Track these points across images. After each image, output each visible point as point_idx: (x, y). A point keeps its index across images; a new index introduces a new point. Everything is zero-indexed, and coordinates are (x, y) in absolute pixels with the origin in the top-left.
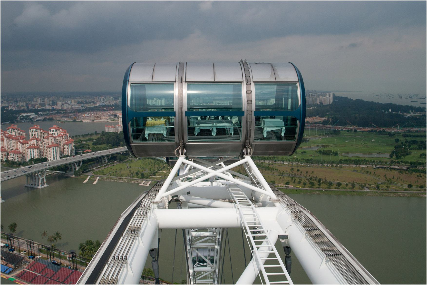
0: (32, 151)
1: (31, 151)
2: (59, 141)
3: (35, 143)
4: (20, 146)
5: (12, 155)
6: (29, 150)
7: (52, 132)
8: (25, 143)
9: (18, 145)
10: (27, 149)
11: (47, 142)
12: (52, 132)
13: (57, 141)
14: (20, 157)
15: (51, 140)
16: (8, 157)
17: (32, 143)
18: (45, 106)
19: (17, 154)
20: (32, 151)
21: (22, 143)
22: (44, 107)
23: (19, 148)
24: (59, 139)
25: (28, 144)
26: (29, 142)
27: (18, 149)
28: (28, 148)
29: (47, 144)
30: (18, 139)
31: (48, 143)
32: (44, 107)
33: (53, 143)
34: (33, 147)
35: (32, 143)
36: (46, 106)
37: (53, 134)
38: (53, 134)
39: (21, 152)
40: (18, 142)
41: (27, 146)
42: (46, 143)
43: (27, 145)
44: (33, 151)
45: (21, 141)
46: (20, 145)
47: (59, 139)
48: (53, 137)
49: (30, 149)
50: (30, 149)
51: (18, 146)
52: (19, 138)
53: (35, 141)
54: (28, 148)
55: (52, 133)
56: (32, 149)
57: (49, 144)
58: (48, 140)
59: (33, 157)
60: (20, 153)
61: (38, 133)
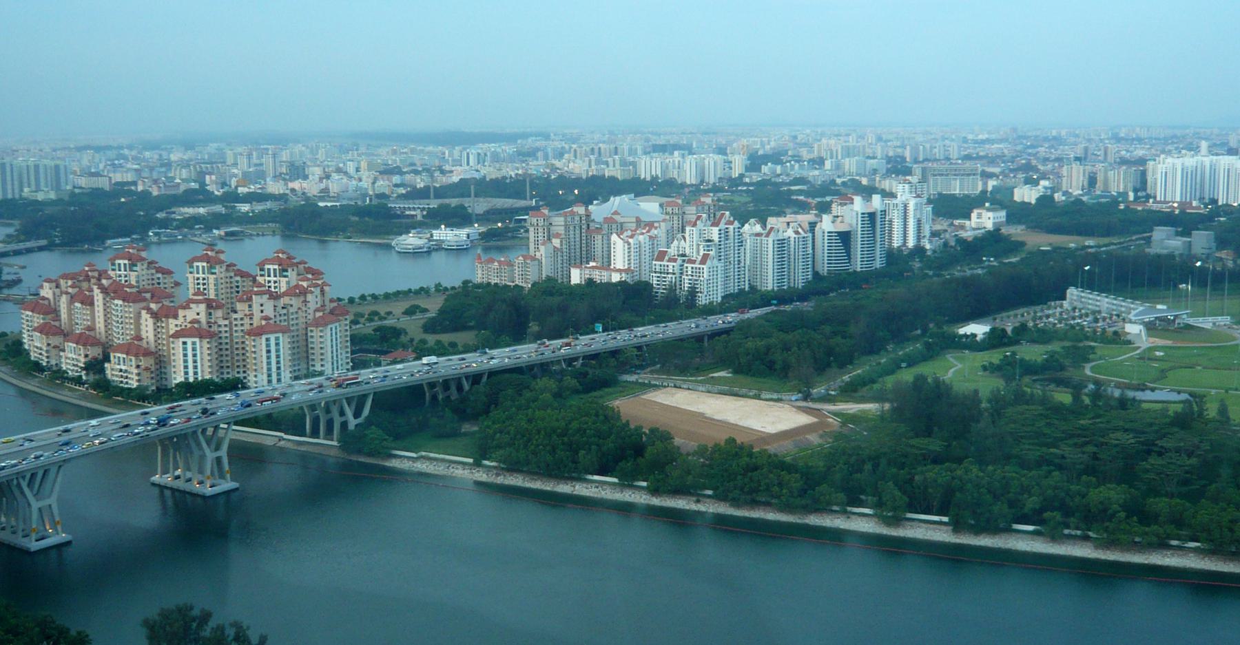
2: (291, 310)
3: (203, 318)
5: (119, 361)
7: (267, 279)
8: (167, 317)
9: (143, 321)
10: (171, 339)
11: (245, 315)
12: (267, 279)
13: (285, 311)
15: (262, 308)
17: (190, 314)
19: (136, 356)
21: (156, 316)
23: (144, 335)
24: (291, 303)
25: (176, 317)
26: (181, 313)
28: (177, 335)
29: (247, 321)
30: (145, 300)
31: (251, 318)
33: (267, 318)
34: (195, 331)
35: (190, 314)
37: (272, 284)
40: (144, 312)
41: (173, 325)
42: (242, 319)
43: (172, 322)
45: (153, 306)
46: (150, 322)
47: (291, 306)
48: (268, 296)
49: (184, 340)
50: (182, 340)
52: (148, 296)
53: (202, 307)
54: (177, 335)
55: (269, 278)
57: (251, 324)
58: (250, 306)
61: (216, 279)
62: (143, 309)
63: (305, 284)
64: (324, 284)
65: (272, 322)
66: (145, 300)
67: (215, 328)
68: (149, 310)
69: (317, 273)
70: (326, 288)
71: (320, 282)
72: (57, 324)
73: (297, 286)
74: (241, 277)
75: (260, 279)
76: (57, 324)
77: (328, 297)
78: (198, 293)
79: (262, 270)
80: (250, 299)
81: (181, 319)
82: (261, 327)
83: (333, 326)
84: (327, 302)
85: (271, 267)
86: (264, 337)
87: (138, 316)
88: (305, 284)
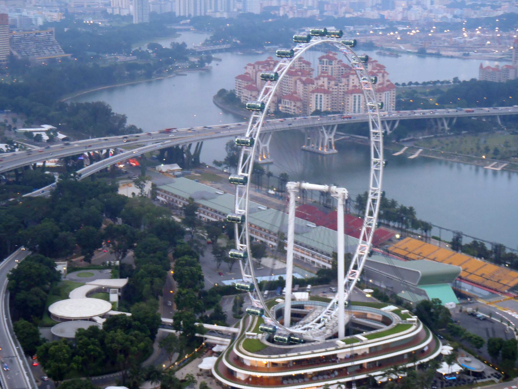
0: (319, 97)
1: (317, 98)
6: (314, 96)
8: (309, 84)
9: (298, 86)
11: (345, 84)
14: (298, 107)
16: (278, 107)
17: (320, 82)
18: (363, 11)
19: (294, 101)
20: (319, 97)
21: (304, 83)
22: (359, 13)
23: (297, 91)
26: (315, 82)
27: (296, 93)
28: (313, 92)
29: (346, 87)
30: (298, 75)
31: (348, 86)
32: (359, 13)
33: (355, 86)
35: (320, 82)
36: (365, 10)
39: (302, 97)
40: (298, 82)
41: (311, 87)
42: (343, 86)
44: (321, 99)
45: (304, 79)
50: (316, 94)
53: (326, 79)
54: (313, 92)
56: (319, 94)
57: (348, 89)
58: (348, 80)
59: (319, 108)
61: (332, 68)
62: (298, 79)
64: (385, 72)
65: (357, 88)
66: (298, 75)
67: (331, 90)
68: (301, 80)
69: (382, 67)
70: (385, 74)
71: (382, 71)
72: (254, 85)
74: (345, 67)
76: (254, 85)
77: (387, 77)
78: (322, 72)
80: (348, 77)
81: (315, 85)
82: (353, 90)
83: (387, 92)
84: (385, 82)
86: (353, 95)
87: (296, 82)
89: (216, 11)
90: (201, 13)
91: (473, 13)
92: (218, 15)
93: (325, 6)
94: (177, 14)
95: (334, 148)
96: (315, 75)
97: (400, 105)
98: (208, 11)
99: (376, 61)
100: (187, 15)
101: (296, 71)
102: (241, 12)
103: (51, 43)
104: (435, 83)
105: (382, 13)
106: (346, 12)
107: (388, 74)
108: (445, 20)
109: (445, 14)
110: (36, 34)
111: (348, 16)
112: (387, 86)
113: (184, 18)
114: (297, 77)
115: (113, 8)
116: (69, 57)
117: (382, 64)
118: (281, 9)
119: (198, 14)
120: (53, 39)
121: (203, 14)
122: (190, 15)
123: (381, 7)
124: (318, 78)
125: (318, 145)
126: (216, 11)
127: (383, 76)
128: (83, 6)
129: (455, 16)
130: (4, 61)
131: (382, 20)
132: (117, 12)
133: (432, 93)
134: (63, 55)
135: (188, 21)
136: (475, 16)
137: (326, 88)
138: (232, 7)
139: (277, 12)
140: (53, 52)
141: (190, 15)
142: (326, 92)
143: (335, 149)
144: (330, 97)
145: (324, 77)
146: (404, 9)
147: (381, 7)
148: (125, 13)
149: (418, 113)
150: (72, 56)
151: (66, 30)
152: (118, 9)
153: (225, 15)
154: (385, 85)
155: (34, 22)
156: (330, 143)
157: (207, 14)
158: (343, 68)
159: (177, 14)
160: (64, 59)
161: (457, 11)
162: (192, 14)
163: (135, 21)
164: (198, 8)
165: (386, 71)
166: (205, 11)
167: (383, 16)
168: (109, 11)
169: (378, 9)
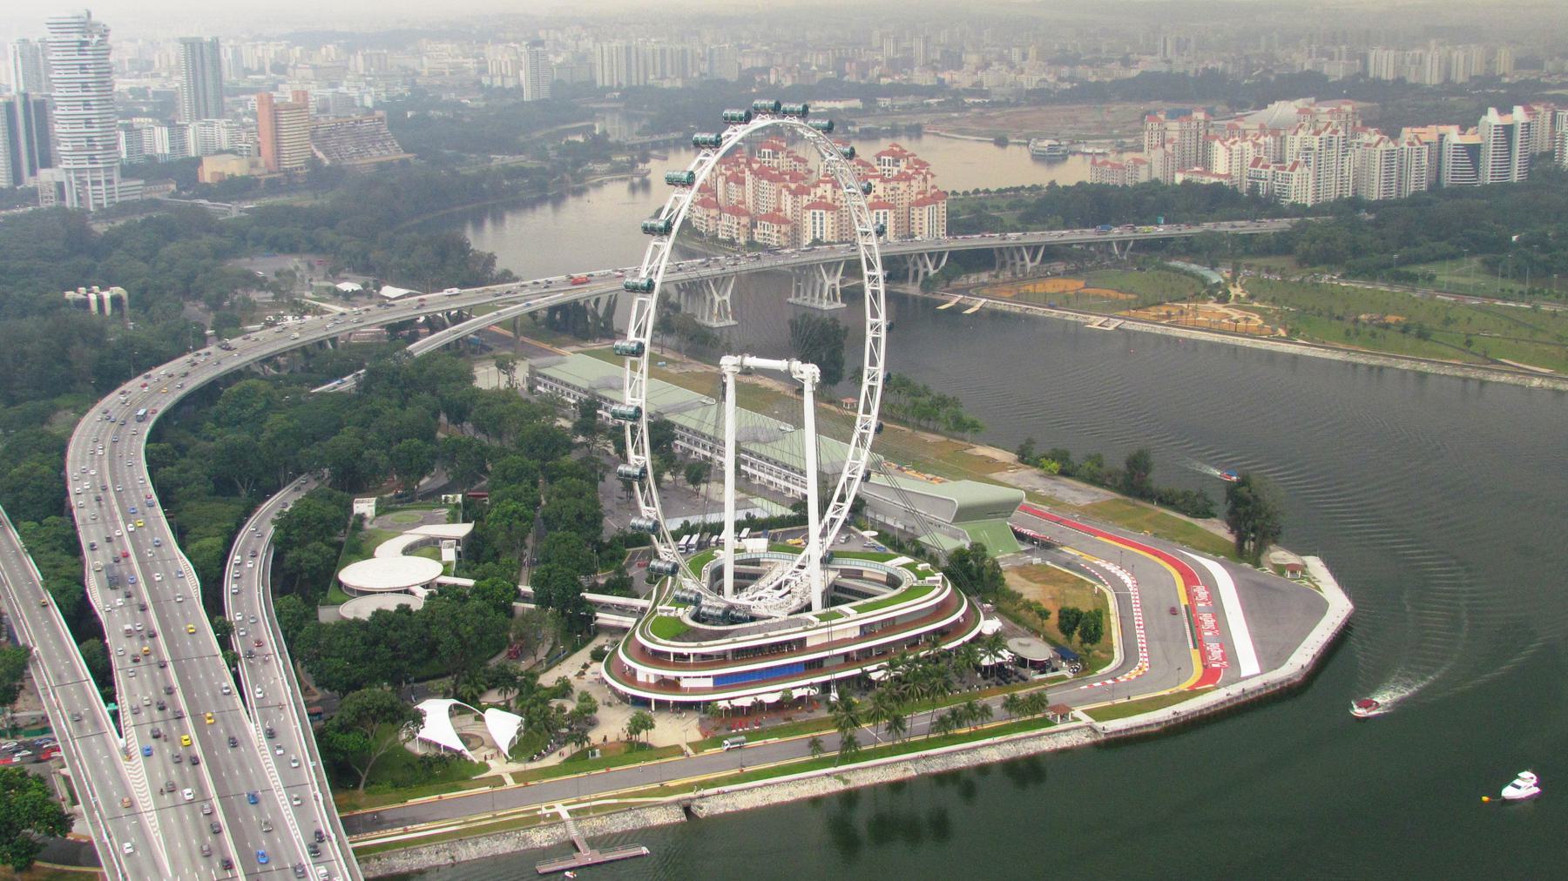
0: (818, 216)
1: (814, 218)
2: (898, 192)
3: (829, 195)
4: (787, 202)
6: (809, 214)
7: (883, 167)
8: (802, 194)
9: (783, 197)
12: (883, 167)
13: (893, 192)
14: (785, 234)
16: (753, 233)
20: (818, 216)
21: (795, 193)
25: (809, 194)
26: (813, 191)
28: (808, 208)
30: (785, 180)
34: (819, 204)
35: (819, 192)
37: (886, 172)
38: (886, 172)
40: (785, 192)
41: (805, 200)
43: (805, 197)
44: (821, 219)
45: (793, 186)
46: (790, 197)
48: (878, 180)
51: (783, 202)
53: (829, 186)
54: (808, 208)
59: (818, 236)
60: (786, 221)
62: (784, 187)
63: (910, 172)
67: (837, 203)
69: (923, 164)
70: (929, 177)
71: (924, 171)
73: (904, 173)
75: (877, 168)
77: (930, 182)
78: (825, 176)
79: (879, 159)
81: (812, 195)
83: (931, 206)
84: (929, 188)
85: (887, 158)
86: (875, 211)
88: (910, 172)
89: (663, 77)
90: (638, 82)
91: (1090, 74)
92: (667, 84)
93: (847, 65)
94: (599, 83)
95: (839, 299)
96: (814, 178)
97: (955, 226)
98: (651, 77)
99: (913, 155)
100: (615, 83)
101: (781, 174)
102: (704, 78)
103: (381, 137)
104: (1017, 190)
105: (941, 76)
106: (880, 76)
107: (933, 176)
108: (1042, 85)
109: (1044, 76)
110: (356, 122)
111: (884, 81)
112: (932, 196)
113: (611, 89)
114: (782, 184)
115: (492, 77)
116: (412, 160)
117: (923, 160)
118: (772, 70)
119: (634, 84)
120: (384, 130)
121: (642, 83)
122: (620, 84)
123: (939, 66)
124: (816, 185)
125: (813, 295)
126: (663, 77)
127: (925, 180)
128: (443, 73)
129: (1061, 79)
130: (301, 168)
131: (939, 88)
132: (498, 82)
133: (1012, 207)
134: (403, 156)
135: (617, 94)
136: (1093, 79)
137: (830, 200)
138: (690, 69)
139: (765, 77)
140: (385, 152)
141: (620, 84)
142: (830, 207)
143: (842, 301)
144: (836, 216)
145: (824, 182)
146: (978, 68)
147: (939, 66)
148: (510, 83)
149: (991, 240)
150: (416, 158)
151: (409, 114)
152: (499, 79)
153: (679, 84)
154: (928, 194)
155: (358, 103)
156: (834, 291)
157: (649, 82)
158: (860, 167)
159: (599, 83)
160: (404, 163)
161: (1065, 71)
162: (624, 83)
163: (527, 97)
164: (634, 74)
165: (932, 170)
166: (646, 77)
167: (942, 81)
168: (486, 81)
169: (935, 69)
